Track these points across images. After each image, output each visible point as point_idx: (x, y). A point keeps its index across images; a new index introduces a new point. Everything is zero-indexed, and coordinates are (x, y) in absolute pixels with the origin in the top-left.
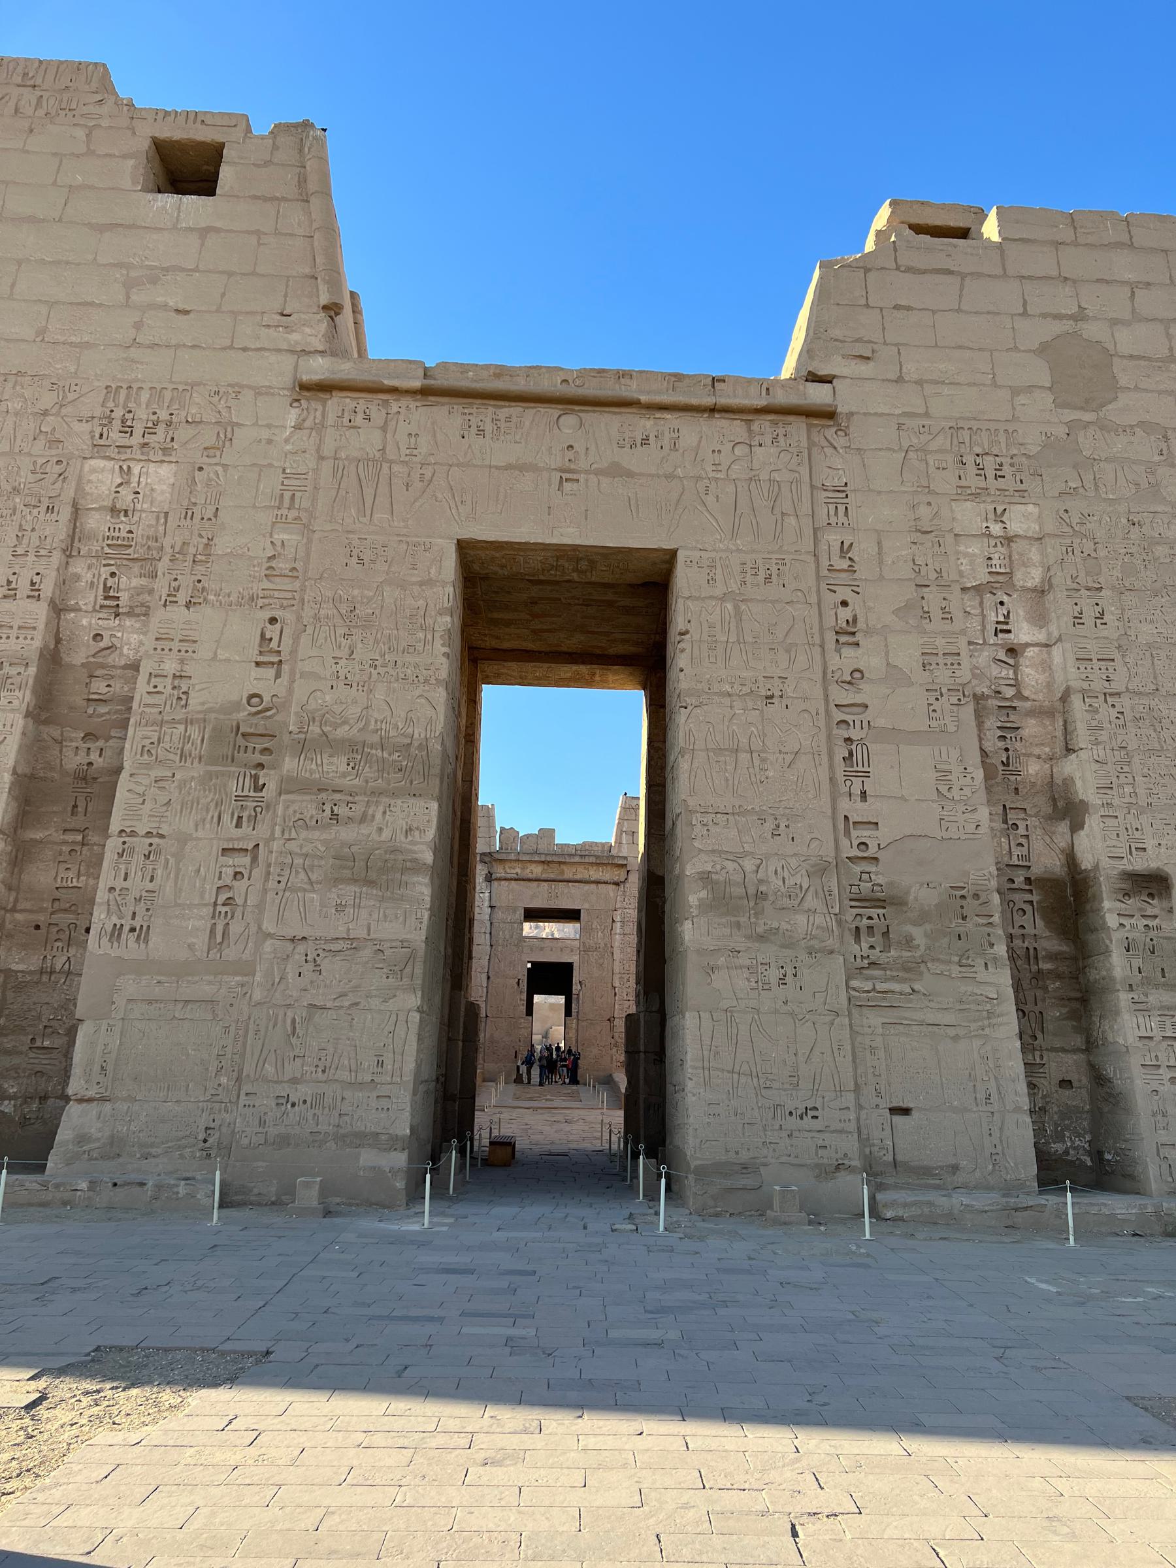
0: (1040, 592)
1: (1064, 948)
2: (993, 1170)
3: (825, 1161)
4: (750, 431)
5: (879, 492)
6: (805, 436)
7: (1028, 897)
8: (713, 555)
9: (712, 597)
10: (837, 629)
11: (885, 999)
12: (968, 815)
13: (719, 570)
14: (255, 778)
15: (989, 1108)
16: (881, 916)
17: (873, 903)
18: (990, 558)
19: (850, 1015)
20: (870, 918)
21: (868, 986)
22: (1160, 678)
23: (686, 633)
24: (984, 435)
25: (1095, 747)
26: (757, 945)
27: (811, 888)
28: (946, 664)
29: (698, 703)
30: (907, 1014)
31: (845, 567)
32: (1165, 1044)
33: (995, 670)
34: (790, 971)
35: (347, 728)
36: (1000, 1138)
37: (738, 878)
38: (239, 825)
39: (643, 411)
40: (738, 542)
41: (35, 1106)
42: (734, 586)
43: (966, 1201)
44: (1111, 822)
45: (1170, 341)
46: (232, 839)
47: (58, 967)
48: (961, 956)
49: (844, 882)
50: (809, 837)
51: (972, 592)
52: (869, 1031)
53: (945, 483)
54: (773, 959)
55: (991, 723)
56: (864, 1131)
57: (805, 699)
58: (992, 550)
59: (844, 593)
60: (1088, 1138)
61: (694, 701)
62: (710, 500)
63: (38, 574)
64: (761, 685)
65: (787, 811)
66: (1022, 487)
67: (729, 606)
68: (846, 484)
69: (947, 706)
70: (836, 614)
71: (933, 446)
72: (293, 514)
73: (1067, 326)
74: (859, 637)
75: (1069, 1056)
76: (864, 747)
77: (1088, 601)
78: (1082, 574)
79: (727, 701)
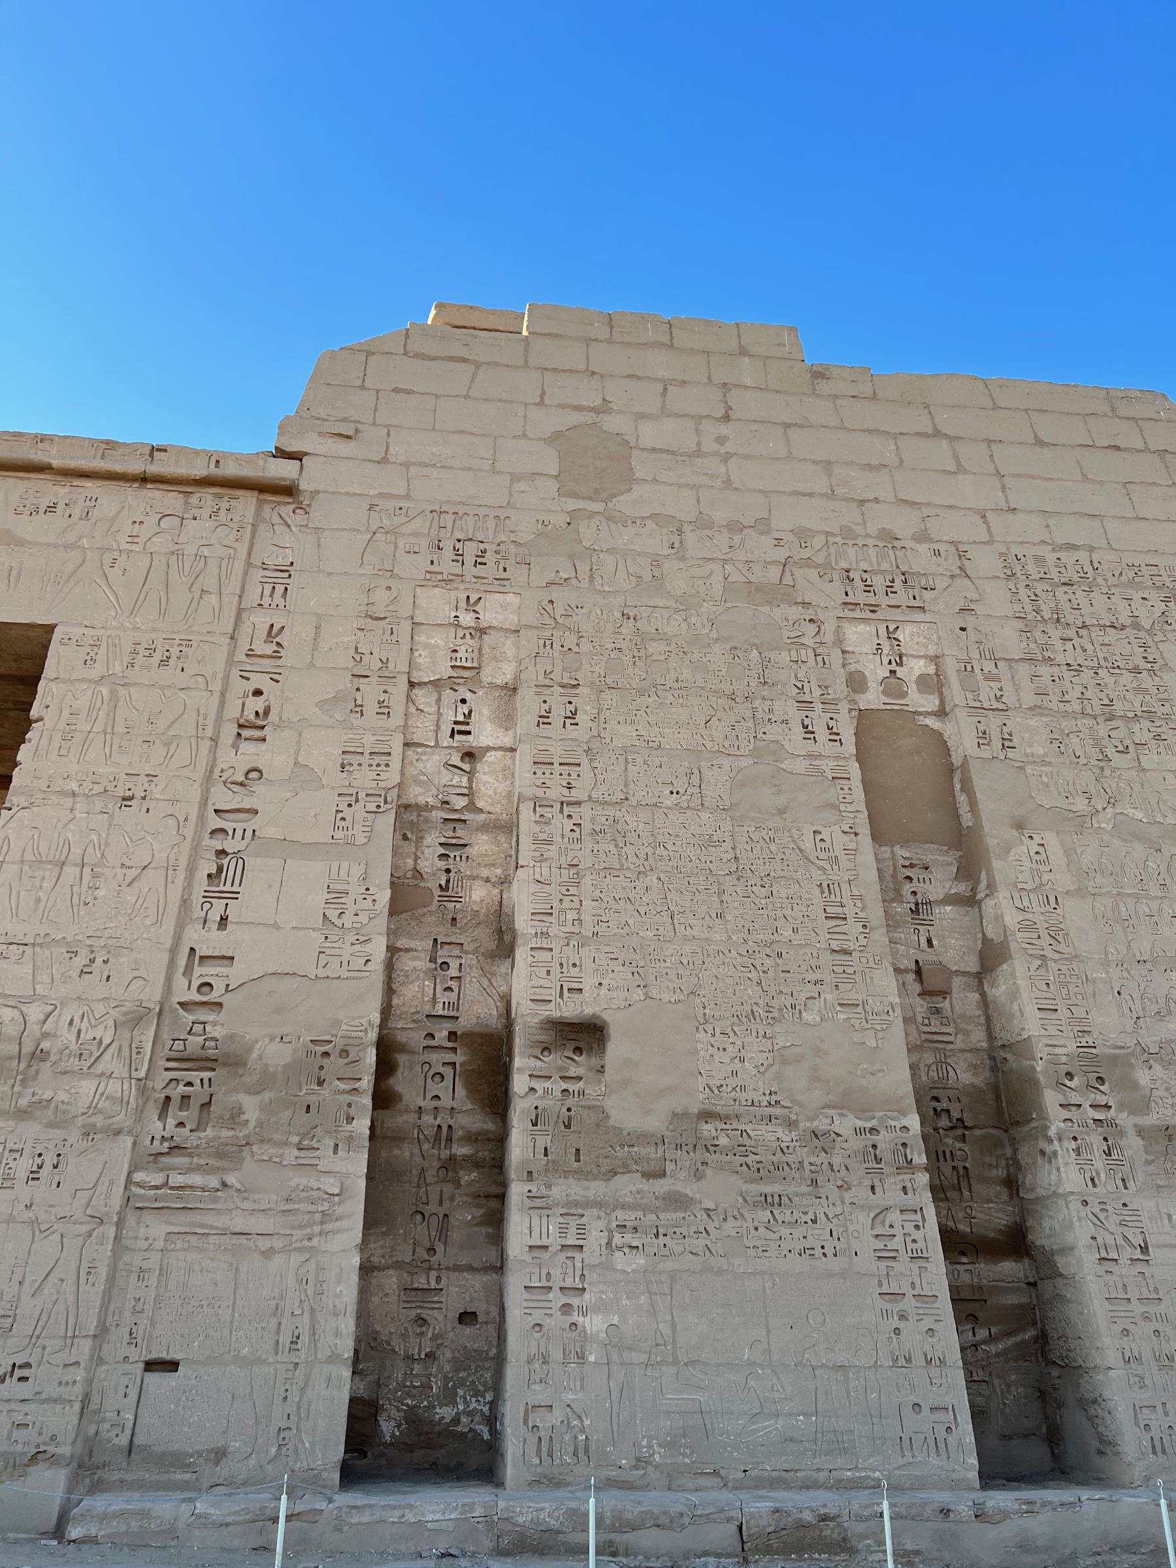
0: (512, 690)
1: (490, 1125)
2: (277, 1456)
3: (19, 1448)
4: (186, 503)
5: (330, 574)
6: (253, 511)
7: (450, 1057)
8: (100, 632)
9: (84, 680)
10: (242, 721)
11: (180, 1198)
12: (357, 947)
13: (103, 649)
16: (206, 1082)
17: (198, 1064)
18: (455, 651)
19: (120, 1224)
21: (157, 1179)
22: (632, 786)
23: (40, 719)
24: (471, 520)
25: (538, 864)
26: (11, 1123)
27: (114, 1044)
29: (26, 804)
30: (207, 1219)
31: (269, 652)
32: (563, 1255)
33: (446, 777)
34: (49, 1160)
36: (299, 1403)
39: (59, 478)
40: (137, 619)
42: (117, 669)
43: (200, 1507)
44: (546, 956)
45: (699, 436)
48: (304, 1136)
49: (166, 1036)
50: (131, 976)
52: (144, 1244)
53: (413, 567)
54: (30, 1144)
55: (433, 840)
56: (95, 1399)
58: (459, 641)
59: (262, 681)
60: (489, 1397)
61: (23, 802)
62: (114, 574)
64: (120, 784)
65: (111, 942)
66: (505, 575)
67: (105, 691)
68: (292, 564)
70: (243, 705)
71: (407, 529)
73: (589, 417)
75: (478, 1277)
76: (240, 861)
77: (559, 698)
78: (558, 670)
79: (68, 802)
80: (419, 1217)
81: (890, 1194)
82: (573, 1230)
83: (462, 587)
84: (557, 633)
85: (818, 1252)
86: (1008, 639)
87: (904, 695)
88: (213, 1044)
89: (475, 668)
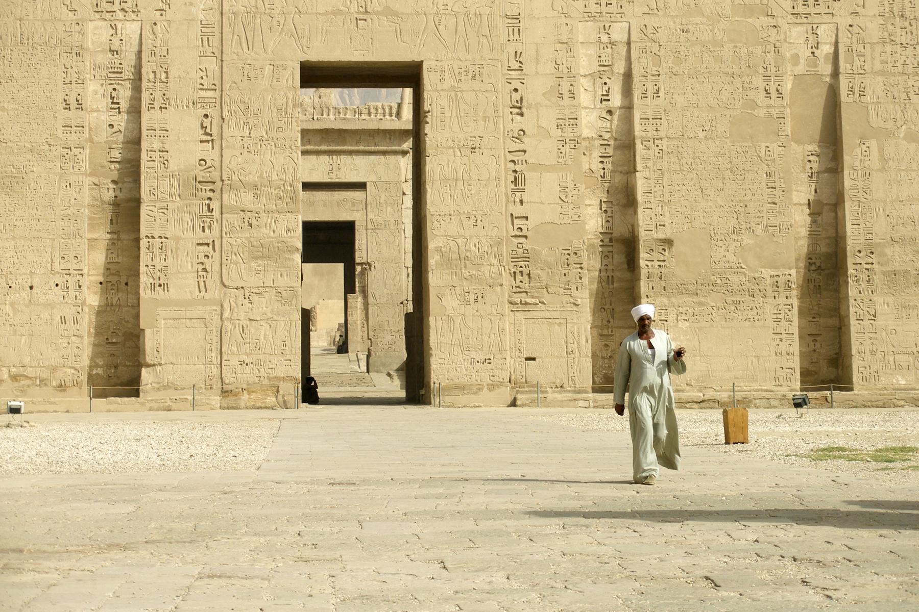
5: (538, 18)
9: (442, 90)
14: (209, 205)
15: (573, 356)
18: (600, 57)
20: (521, 267)
23: (429, 112)
28: (569, 125)
33: (601, 124)
34: (480, 295)
35: (251, 176)
37: (455, 249)
38: (204, 231)
41: (113, 371)
46: (200, 238)
47: (114, 303)
51: (589, 77)
57: (492, 149)
59: (516, 84)
62: (441, 28)
63: (79, 95)
67: (453, 94)
69: (568, 150)
72: (211, 50)
74: (524, 110)
75: (626, 330)
80: (603, 310)
81: (782, 300)
82: (663, 314)
83: (601, 19)
84: (649, 44)
85: (752, 320)
86: (873, 30)
87: (816, 65)
88: (526, 251)
89: (610, 65)
